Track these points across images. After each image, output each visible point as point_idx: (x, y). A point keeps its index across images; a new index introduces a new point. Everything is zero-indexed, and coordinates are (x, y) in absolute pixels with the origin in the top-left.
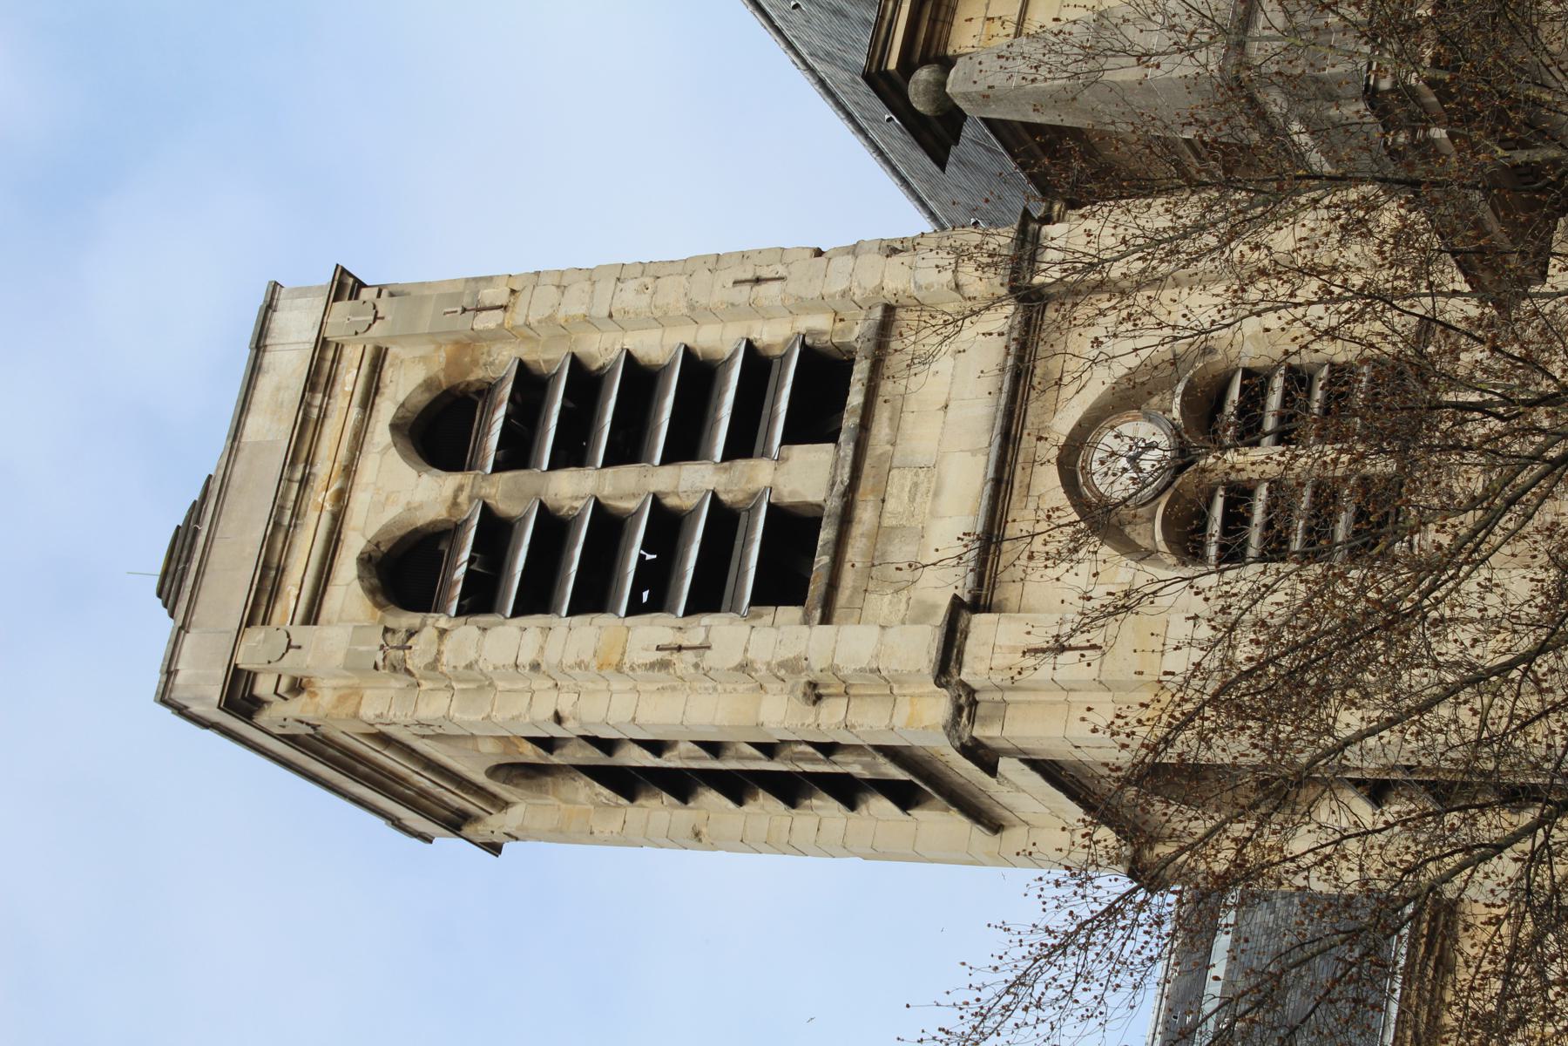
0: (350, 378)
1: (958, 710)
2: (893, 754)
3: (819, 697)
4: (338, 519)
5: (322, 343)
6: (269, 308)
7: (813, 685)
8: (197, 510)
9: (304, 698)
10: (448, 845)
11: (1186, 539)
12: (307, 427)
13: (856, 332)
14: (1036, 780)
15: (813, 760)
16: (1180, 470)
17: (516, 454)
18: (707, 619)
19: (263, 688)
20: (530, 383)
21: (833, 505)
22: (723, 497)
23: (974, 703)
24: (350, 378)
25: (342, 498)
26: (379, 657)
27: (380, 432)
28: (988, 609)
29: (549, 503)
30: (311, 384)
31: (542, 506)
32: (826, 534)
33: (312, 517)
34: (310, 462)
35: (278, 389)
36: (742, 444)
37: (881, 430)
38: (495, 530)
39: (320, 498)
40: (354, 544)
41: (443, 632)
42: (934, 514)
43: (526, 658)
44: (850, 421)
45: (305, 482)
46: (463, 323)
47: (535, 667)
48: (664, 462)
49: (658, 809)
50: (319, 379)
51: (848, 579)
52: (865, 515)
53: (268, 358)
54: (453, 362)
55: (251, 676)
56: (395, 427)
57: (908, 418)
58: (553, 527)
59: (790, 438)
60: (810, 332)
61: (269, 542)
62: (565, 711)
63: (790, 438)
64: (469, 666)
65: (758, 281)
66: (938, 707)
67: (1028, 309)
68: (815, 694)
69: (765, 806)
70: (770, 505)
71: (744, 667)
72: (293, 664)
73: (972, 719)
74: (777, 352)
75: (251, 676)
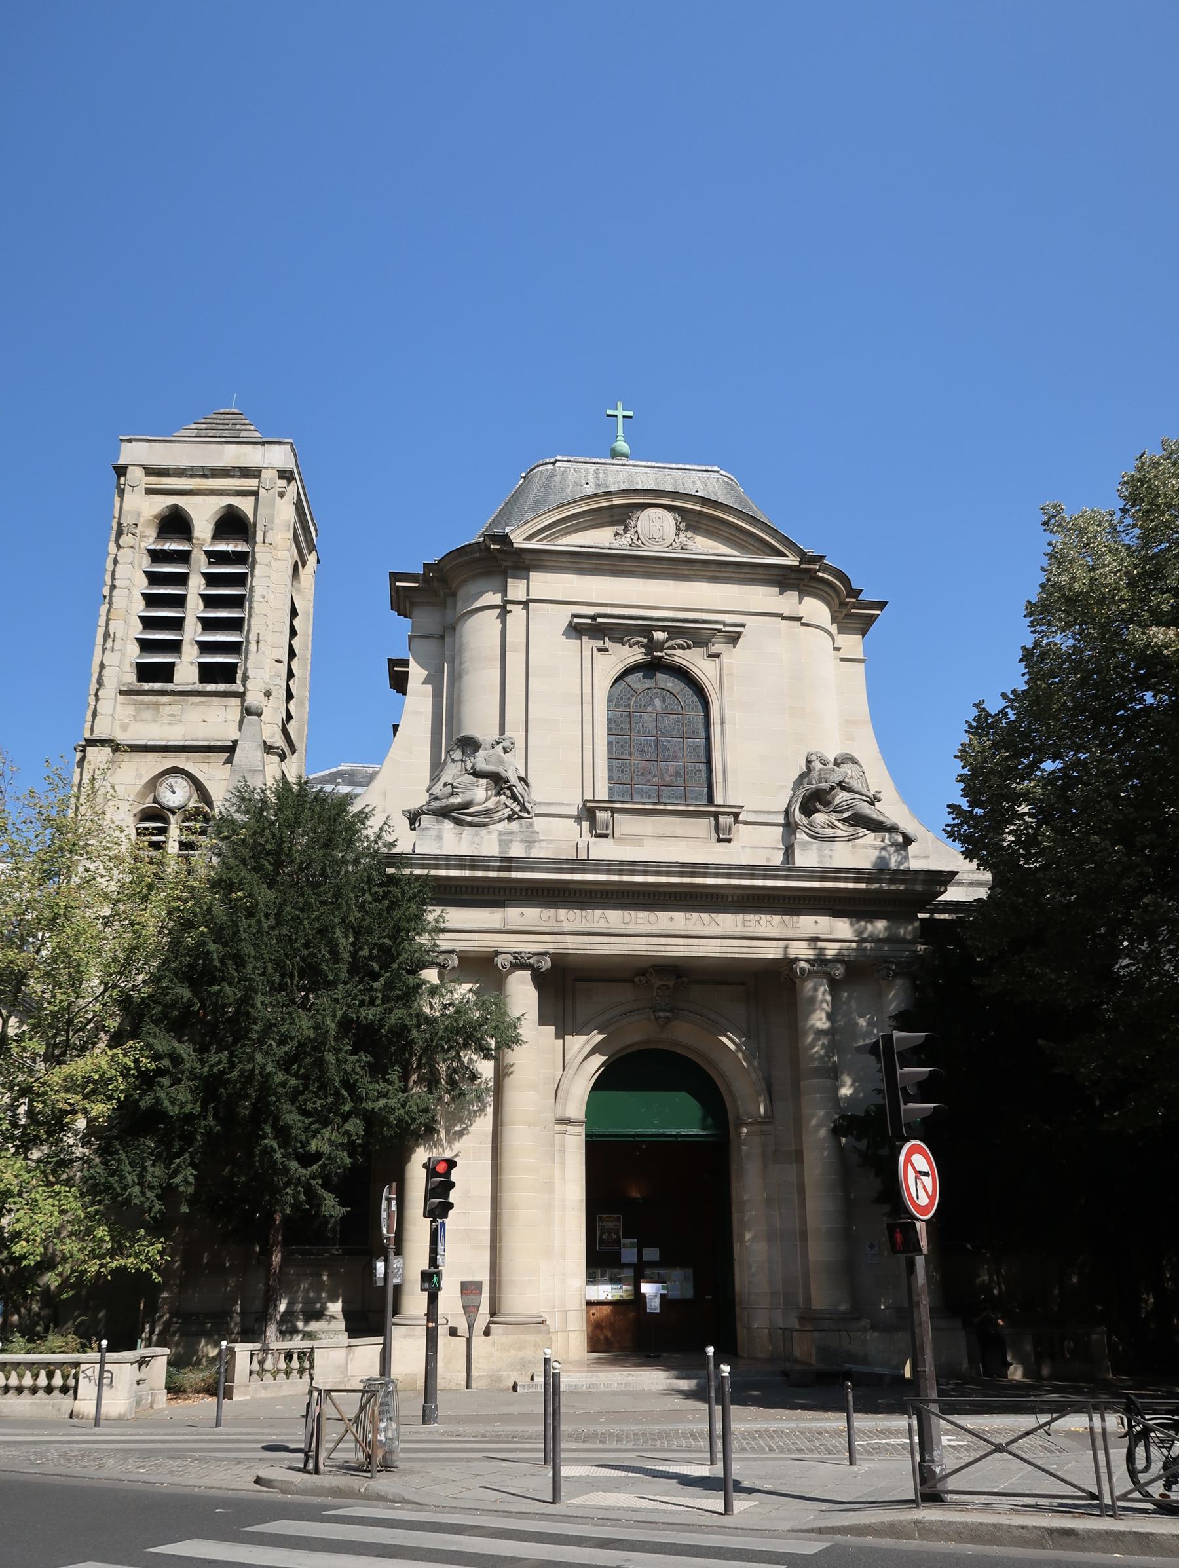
0: (250, 484)
11: (147, 815)
17: (216, 557)
29: (191, 576)
41: (132, 547)
56: (229, 506)
58: (181, 580)
65: (258, 642)
70: (172, 664)
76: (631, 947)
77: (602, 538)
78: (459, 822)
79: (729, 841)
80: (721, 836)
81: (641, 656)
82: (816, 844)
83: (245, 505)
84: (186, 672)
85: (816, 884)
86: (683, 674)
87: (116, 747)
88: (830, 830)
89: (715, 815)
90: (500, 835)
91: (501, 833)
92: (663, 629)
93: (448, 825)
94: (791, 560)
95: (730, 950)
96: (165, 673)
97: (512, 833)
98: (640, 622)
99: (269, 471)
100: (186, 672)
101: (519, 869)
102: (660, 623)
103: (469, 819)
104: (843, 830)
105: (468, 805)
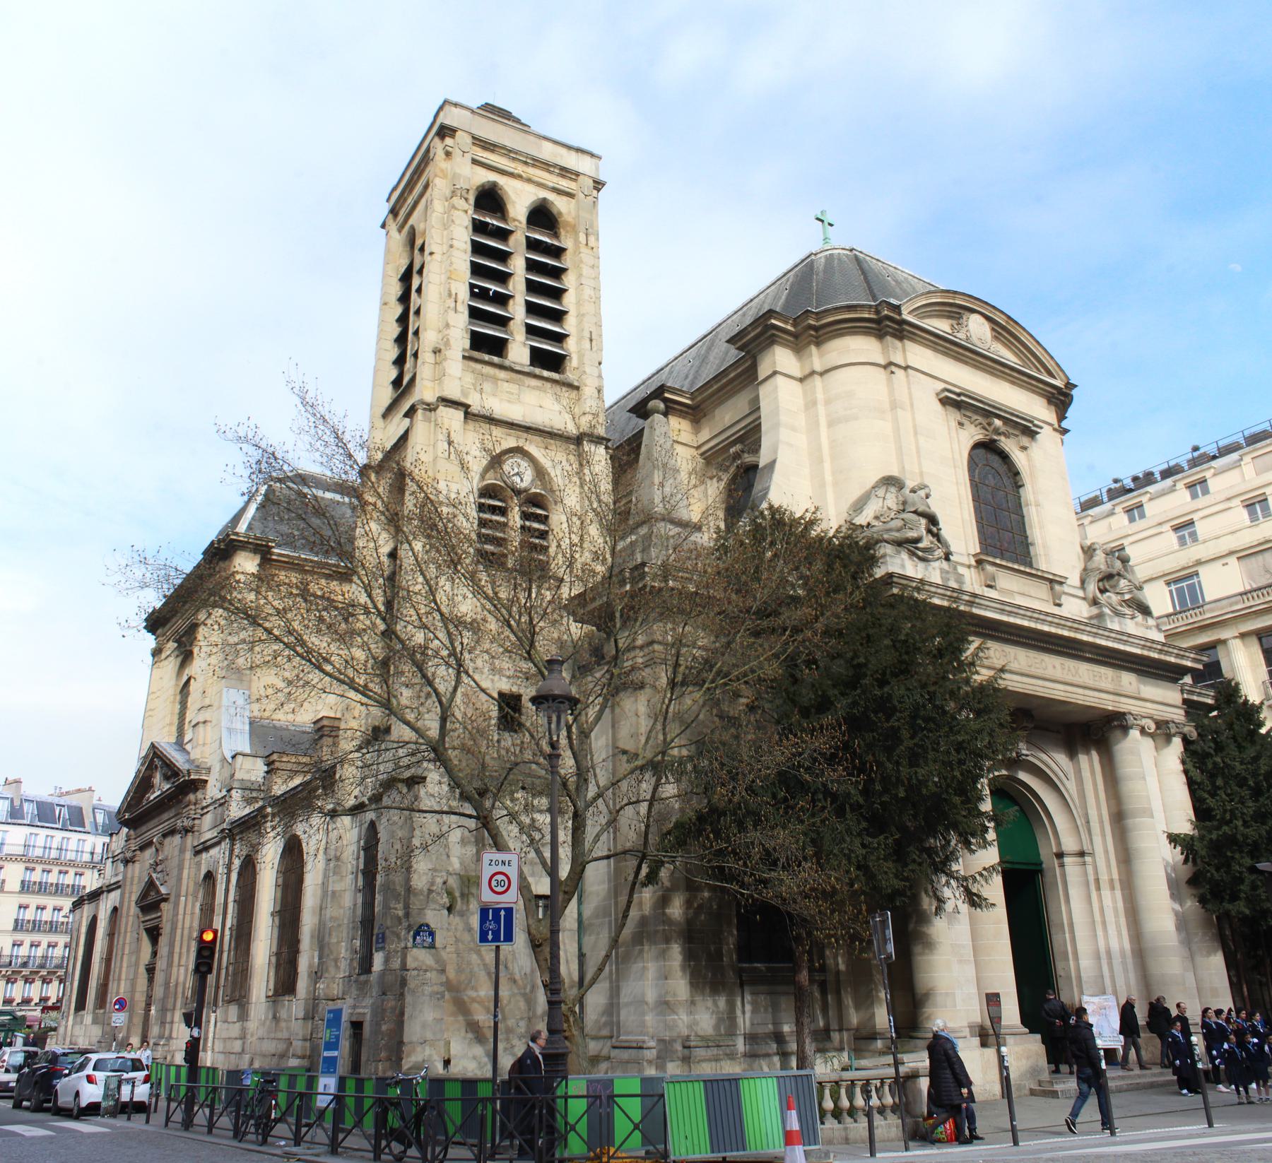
0: (564, 184)
1: (428, 405)
2: (413, 379)
3: (435, 353)
4: (511, 175)
5: (577, 174)
6: (592, 155)
7: (440, 351)
8: (518, 121)
9: (444, 156)
10: (385, 208)
11: (487, 492)
12: (546, 166)
13: (570, 375)
14: (401, 432)
15: (412, 350)
16: (513, 490)
17: (532, 245)
18: (467, 313)
19: (448, 141)
20: (557, 252)
21: (507, 363)
22: (512, 322)
23: (430, 410)
24: (564, 184)
25: (519, 177)
26: (458, 187)
27: (543, 194)
28: (465, 418)
29: (513, 256)
30: (563, 169)
31: (512, 253)
32: (496, 359)
33: (513, 165)
34: (533, 166)
35: (562, 156)
36: (531, 331)
37: (534, 382)
38: (503, 235)
39: (519, 169)
40: (501, 180)
41: (466, 212)
42: (501, 400)
43: (455, 243)
44: (537, 371)
45: (526, 163)
46: (582, 228)
47: (451, 246)
48: (526, 301)
49: (396, 289)
50: (565, 172)
51: (478, 366)
52: (502, 374)
53: (573, 153)
54: (567, 224)
55: (453, 136)
56: (545, 200)
57: (537, 393)
58: (503, 257)
59: (533, 349)
60: (571, 358)
61: (504, 147)
62: (434, 256)
63: (533, 349)
64: (453, 221)
65: (591, 340)
66: (430, 397)
67: (574, 439)
68: (436, 351)
69: (396, 330)
70: (507, 340)
71: (447, 326)
72: (457, 153)
73: (425, 409)
74: (565, 345)
75: (453, 136)
76: (1034, 688)
77: (941, 326)
78: (912, 554)
79: (1059, 605)
80: (1058, 601)
81: (981, 437)
82: (1116, 619)
83: (560, 205)
84: (519, 352)
85: (1138, 651)
86: (1004, 457)
87: (469, 415)
88: (1119, 608)
89: (1051, 581)
90: (941, 573)
91: (942, 570)
92: (999, 417)
93: (905, 556)
94: (1059, 383)
95: (1088, 699)
96: (497, 347)
97: (948, 572)
98: (987, 407)
99: (586, 178)
100: (519, 352)
101: (980, 606)
102: (997, 412)
103: (920, 553)
104: (1127, 611)
105: (918, 540)
